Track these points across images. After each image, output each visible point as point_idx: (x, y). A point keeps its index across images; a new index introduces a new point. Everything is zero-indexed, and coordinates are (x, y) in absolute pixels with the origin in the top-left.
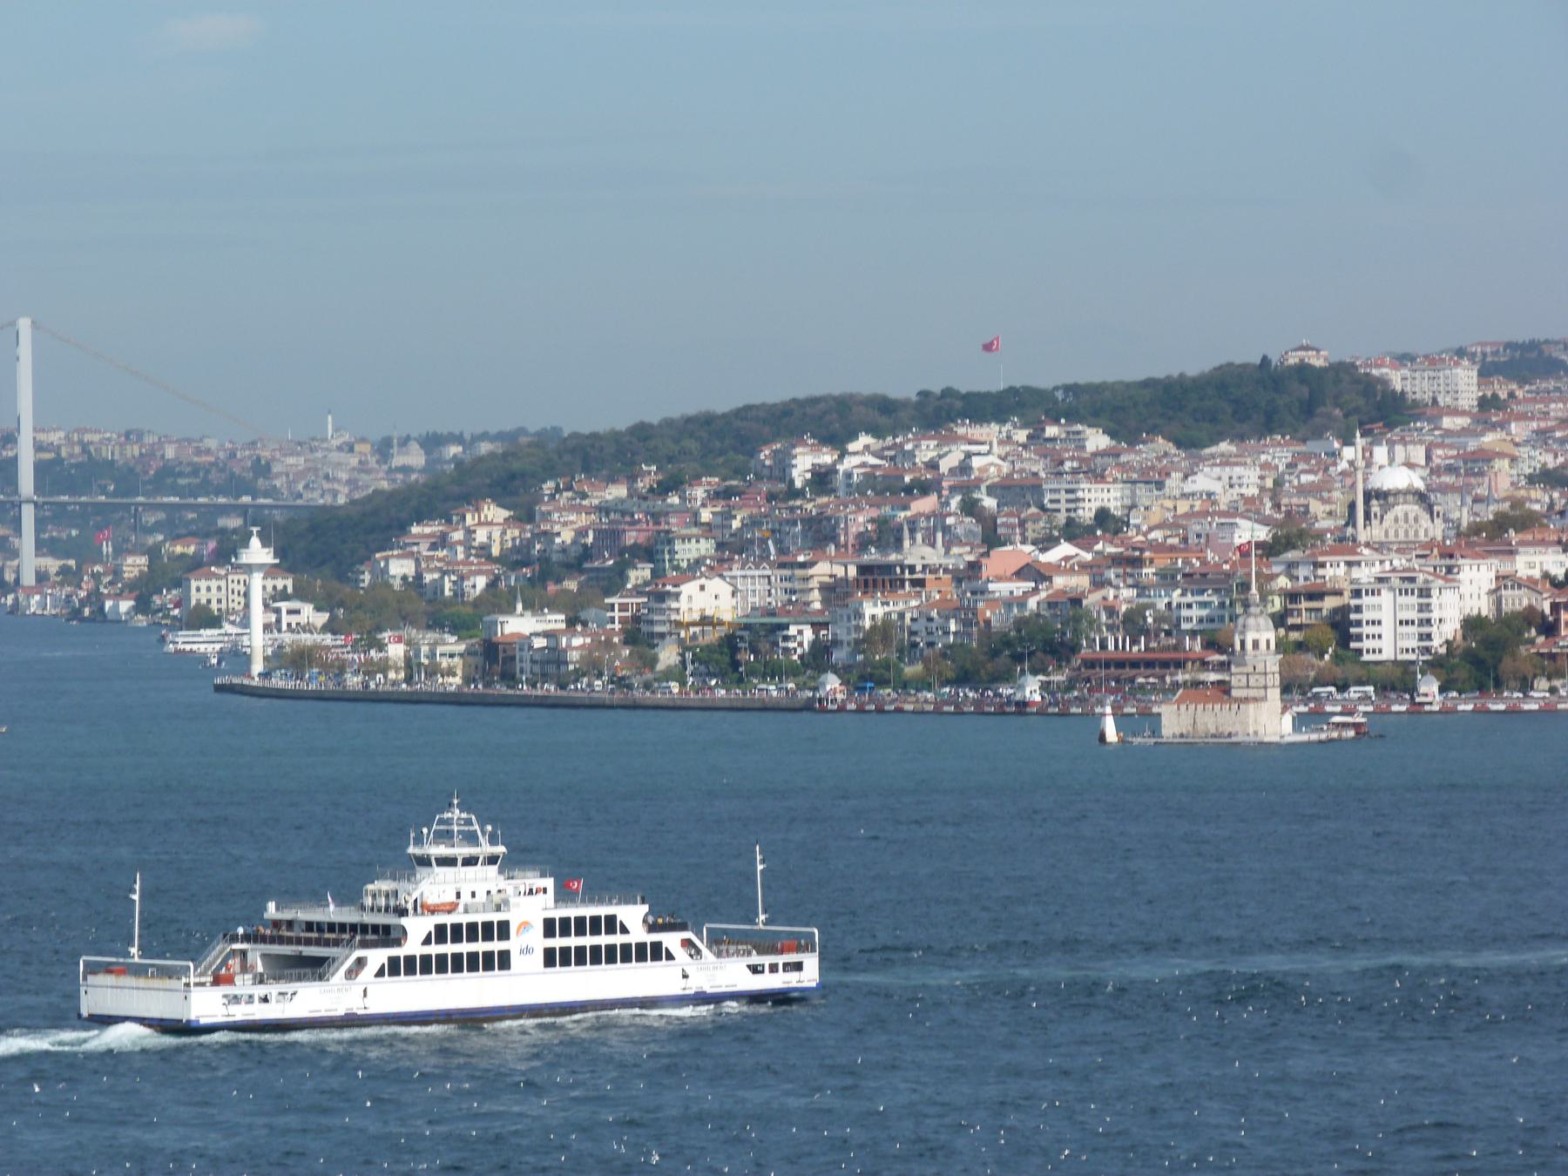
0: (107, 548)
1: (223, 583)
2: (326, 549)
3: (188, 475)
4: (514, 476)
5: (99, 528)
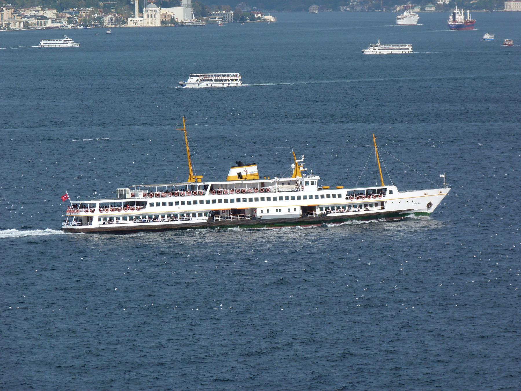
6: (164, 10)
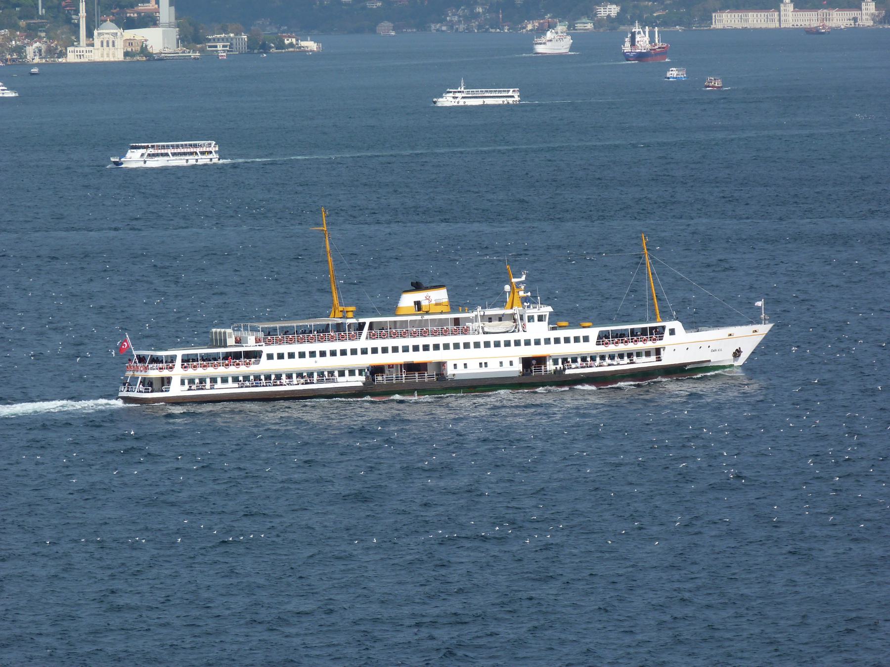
6: (129, 34)
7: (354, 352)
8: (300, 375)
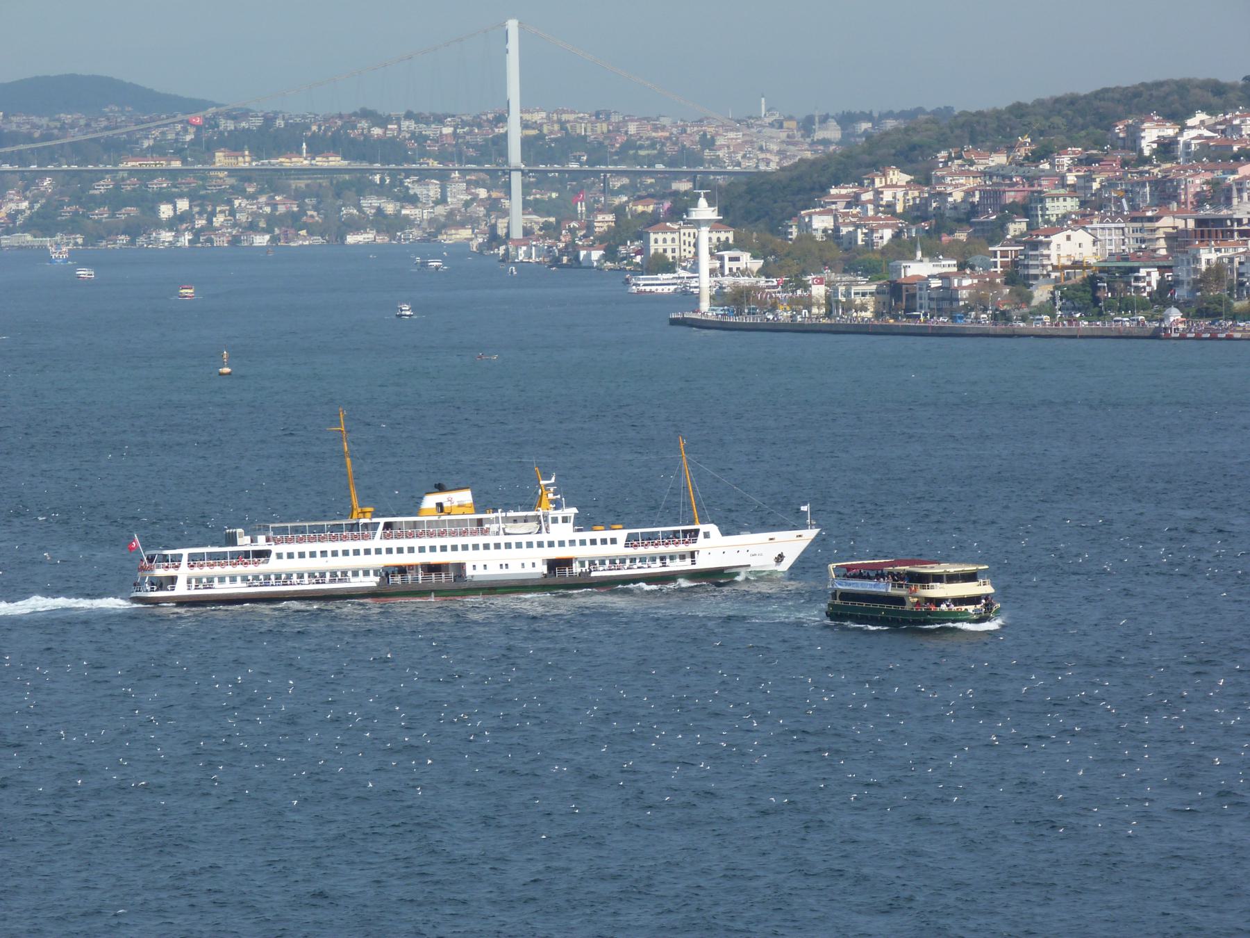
0: (581, 208)
1: (676, 236)
2: (758, 208)
3: (648, 148)
4: (912, 148)
5: (577, 192)
7: (367, 552)
8: (311, 575)
